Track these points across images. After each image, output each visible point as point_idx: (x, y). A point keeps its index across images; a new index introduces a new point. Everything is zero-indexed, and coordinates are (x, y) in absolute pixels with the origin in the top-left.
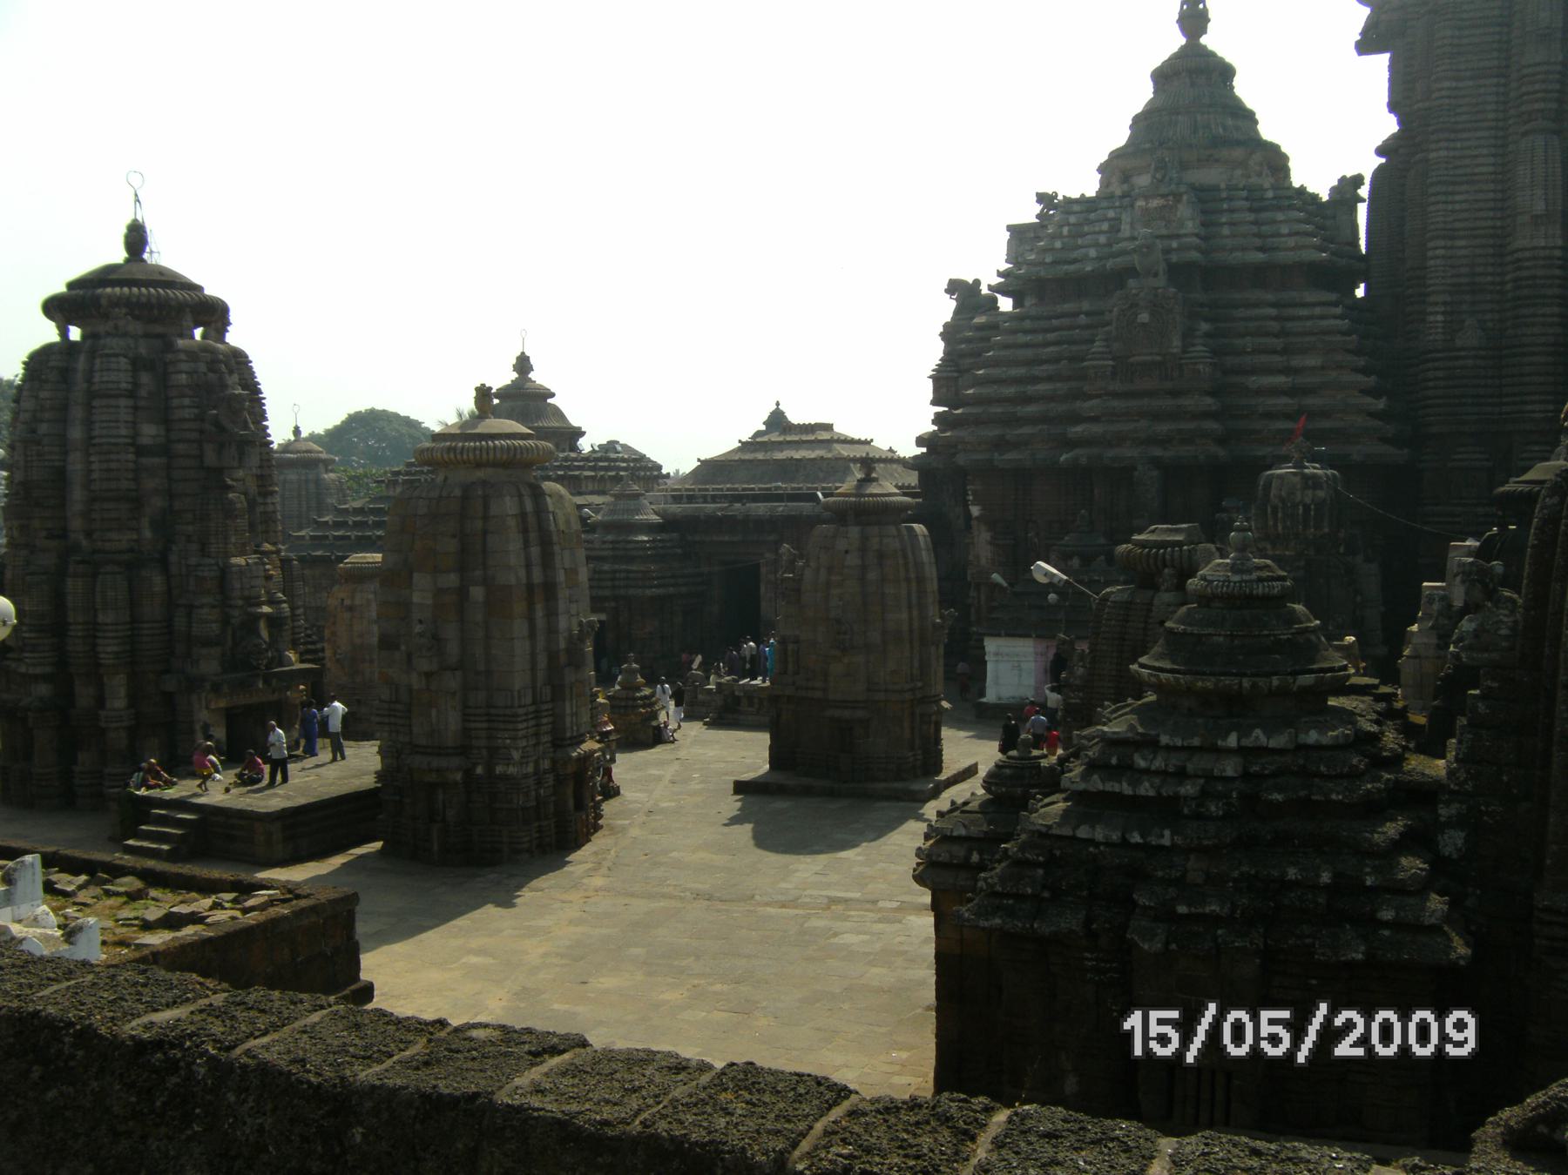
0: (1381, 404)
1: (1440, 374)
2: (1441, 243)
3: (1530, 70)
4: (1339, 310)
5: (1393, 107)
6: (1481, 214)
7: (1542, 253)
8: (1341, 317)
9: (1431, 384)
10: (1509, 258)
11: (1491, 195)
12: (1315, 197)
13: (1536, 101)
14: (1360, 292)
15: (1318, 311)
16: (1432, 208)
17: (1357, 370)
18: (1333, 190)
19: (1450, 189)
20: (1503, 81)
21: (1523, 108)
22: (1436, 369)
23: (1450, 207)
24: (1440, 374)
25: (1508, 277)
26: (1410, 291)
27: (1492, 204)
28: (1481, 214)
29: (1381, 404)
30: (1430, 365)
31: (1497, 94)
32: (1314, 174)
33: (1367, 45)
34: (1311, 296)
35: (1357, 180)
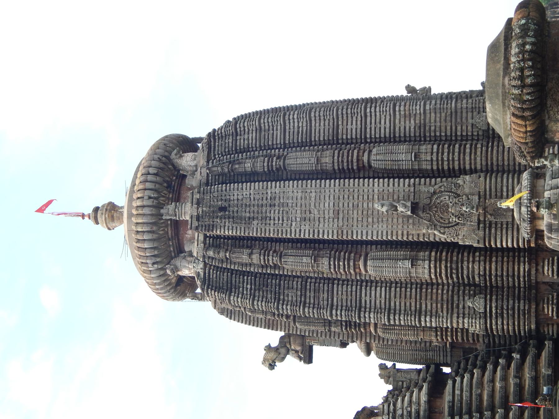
0: (516, 356)
1: (499, 323)
2: (423, 319)
3: (332, 267)
4: (458, 379)
5: (344, 345)
6: (408, 293)
7: (433, 262)
8: (462, 378)
9: (505, 327)
10: (434, 281)
11: (398, 289)
12: (389, 392)
13: (349, 264)
14: (447, 370)
15: (457, 392)
16: (402, 323)
17: (495, 371)
18: (387, 382)
19: (392, 311)
20: (336, 282)
21: (352, 271)
22: (497, 324)
23: (403, 312)
24: (499, 323)
25: (445, 282)
26: (449, 339)
27: (403, 289)
28: (408, 293)
29: (516, 356)
30: (494, 327)
31: (343, 285)
32: (376, 392)
33: (308, 358)
34: (447, 397)
35: (382, 367)
